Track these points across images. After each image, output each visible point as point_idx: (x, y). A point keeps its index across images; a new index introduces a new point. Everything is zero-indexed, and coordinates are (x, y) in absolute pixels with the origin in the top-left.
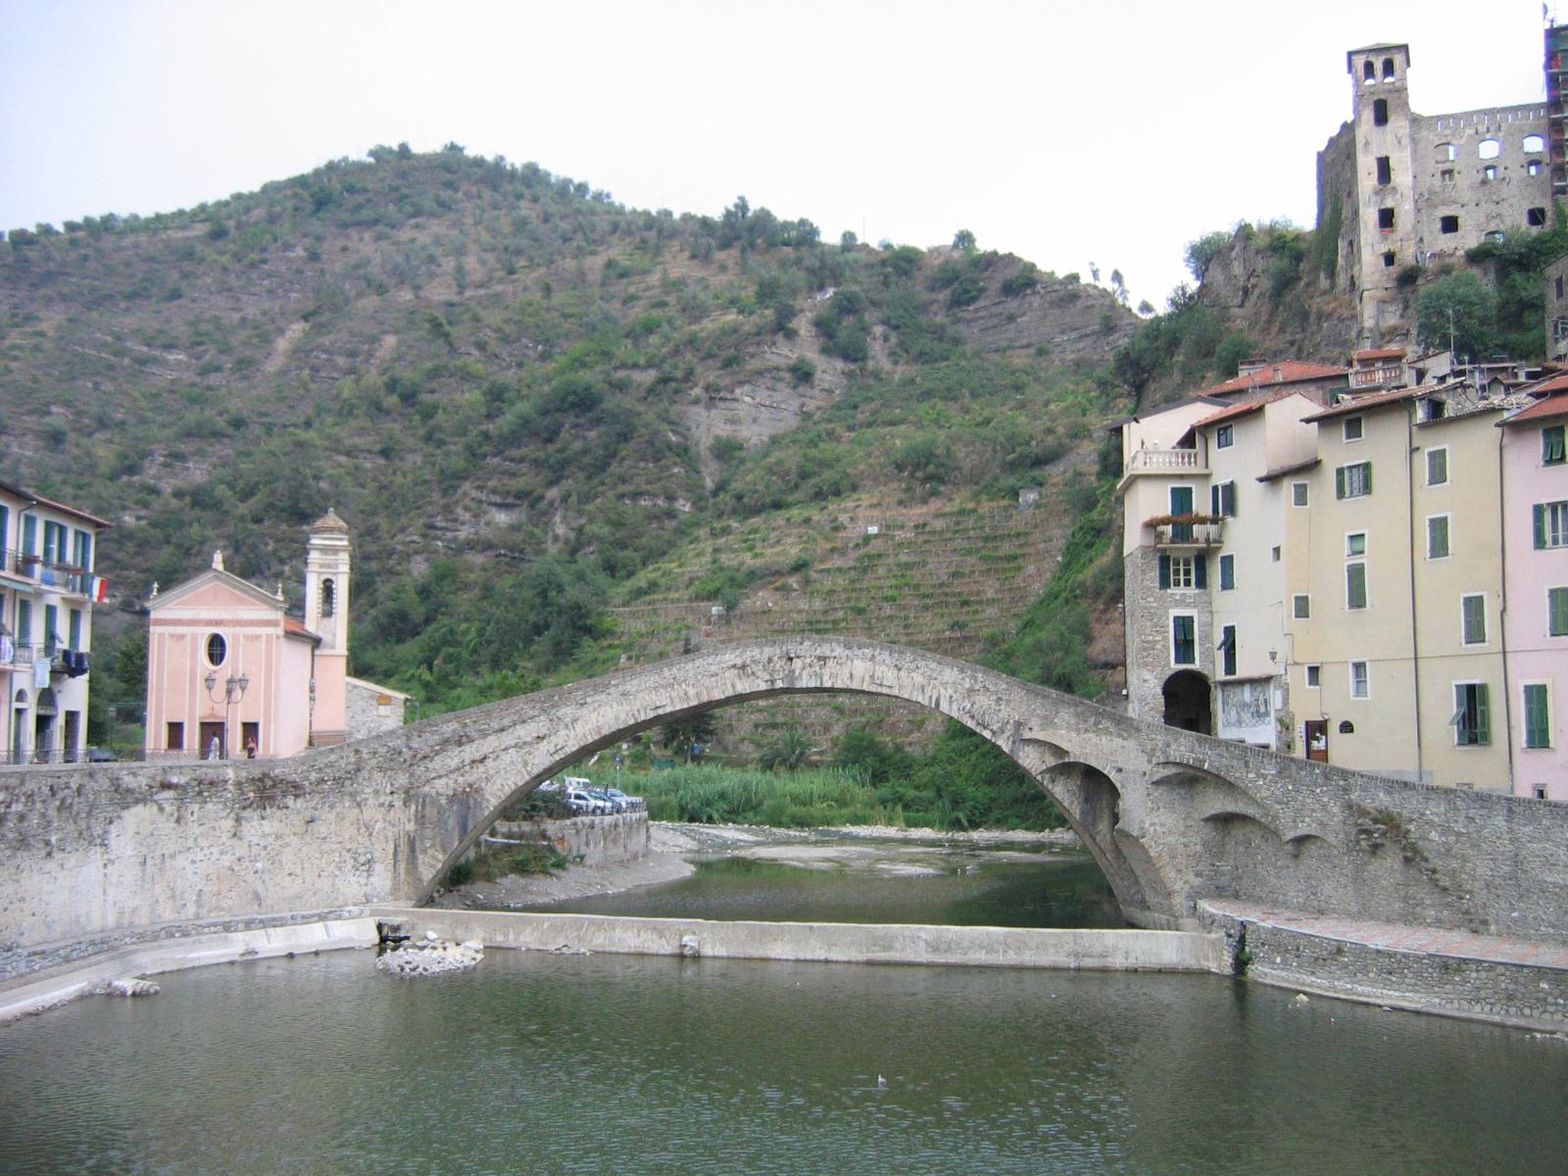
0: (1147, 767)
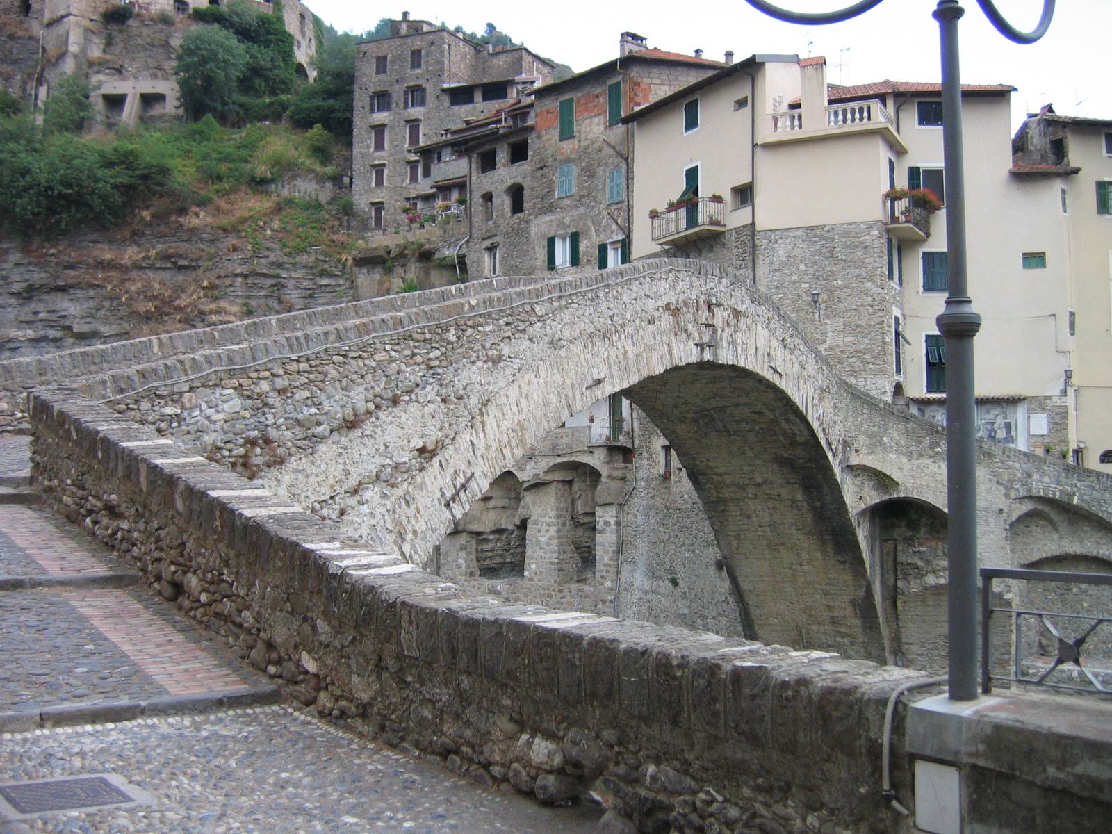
0: (1003, 503)
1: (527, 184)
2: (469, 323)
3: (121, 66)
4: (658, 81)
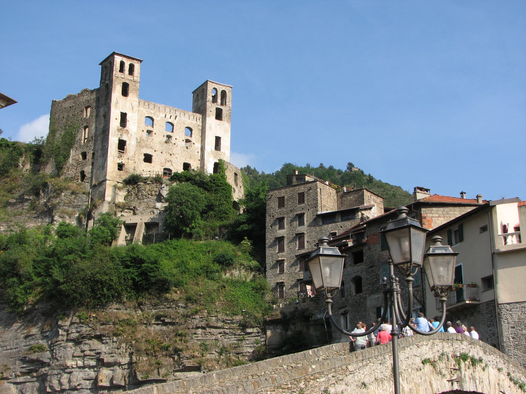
1: (363, 276)
2: (312, 378)
3: (134, 207)
4: (437, 215)
